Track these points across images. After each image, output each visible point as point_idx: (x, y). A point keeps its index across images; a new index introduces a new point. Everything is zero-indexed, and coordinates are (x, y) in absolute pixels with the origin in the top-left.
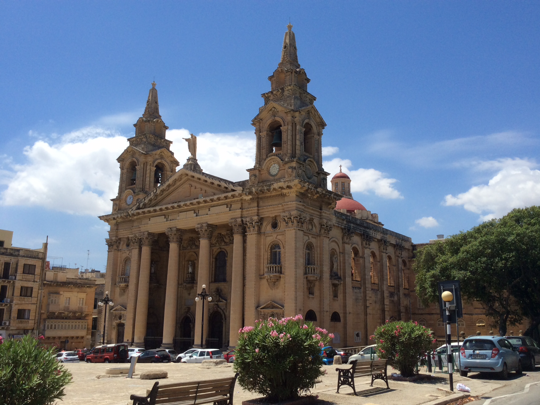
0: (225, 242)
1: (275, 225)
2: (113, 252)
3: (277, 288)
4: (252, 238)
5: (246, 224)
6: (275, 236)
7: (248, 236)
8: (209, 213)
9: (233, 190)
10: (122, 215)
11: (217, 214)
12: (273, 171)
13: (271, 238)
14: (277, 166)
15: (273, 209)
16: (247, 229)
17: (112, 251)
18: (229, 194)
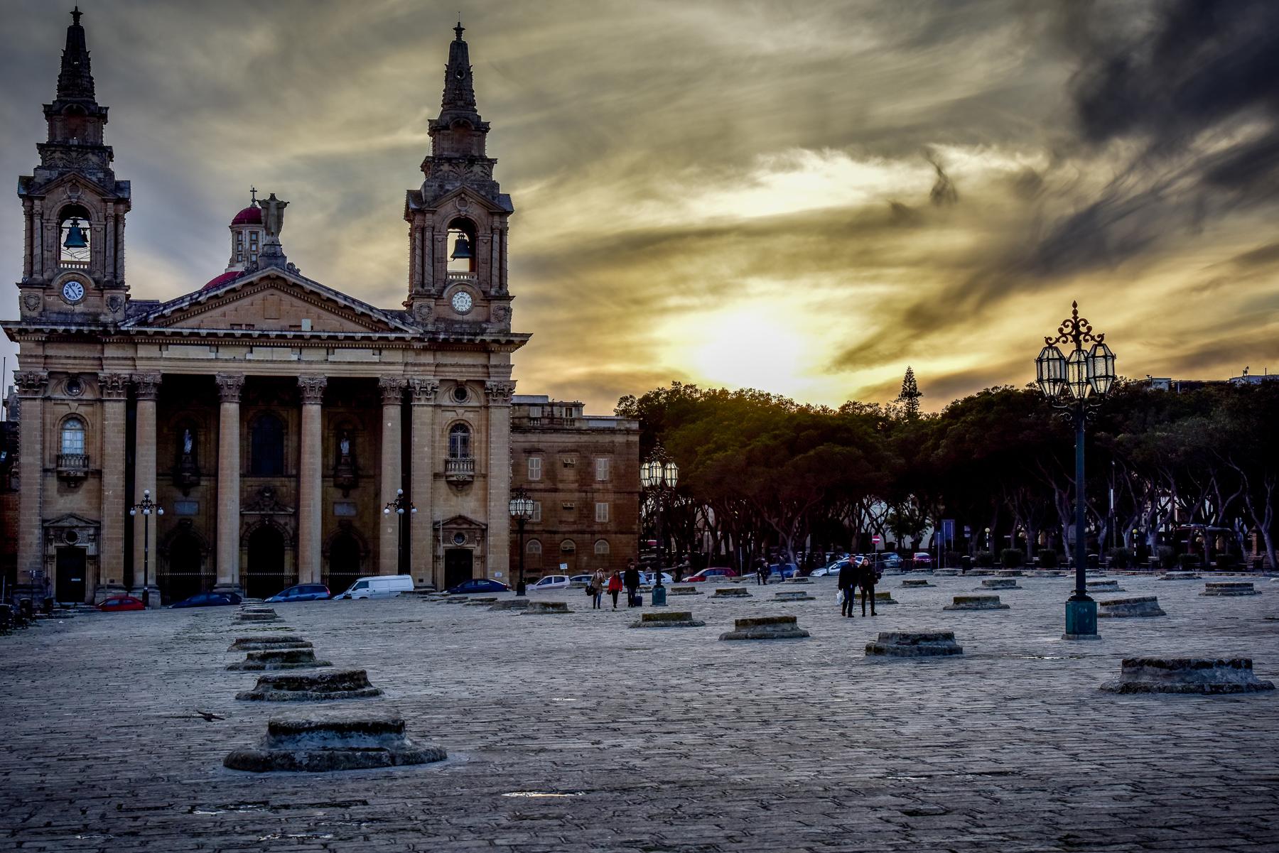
1: (461, 393)
2: (38, 402)
3: (467, 495)
4: (422, 414)
5: (414, 388)
6: (460, 411)
7: (415, 409)
8: (331, 358)
9: (401, 331)
10: (85, 329)
12: (460, 304)
13: (454, 413)
14: (467, 296)
15: (464, 369)
16: (415, 396)
17: (35, 399)
18: (393, 335)
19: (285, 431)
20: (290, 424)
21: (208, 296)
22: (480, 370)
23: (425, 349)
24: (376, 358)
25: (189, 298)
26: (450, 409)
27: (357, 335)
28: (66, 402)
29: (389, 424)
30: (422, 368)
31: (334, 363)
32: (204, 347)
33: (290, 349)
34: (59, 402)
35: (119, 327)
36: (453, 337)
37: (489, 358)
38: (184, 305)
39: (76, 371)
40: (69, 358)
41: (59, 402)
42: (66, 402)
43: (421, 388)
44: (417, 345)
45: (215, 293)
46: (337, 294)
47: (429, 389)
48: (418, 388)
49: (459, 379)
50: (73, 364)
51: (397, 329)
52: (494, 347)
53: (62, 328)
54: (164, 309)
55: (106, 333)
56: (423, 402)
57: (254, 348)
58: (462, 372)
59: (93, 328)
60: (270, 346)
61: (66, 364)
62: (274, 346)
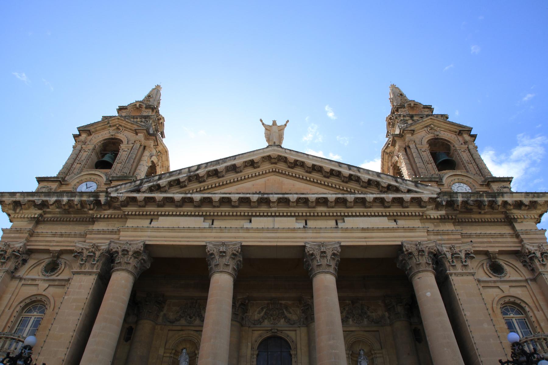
0: (285, 318)
6: (505, 287)
11: (363, 230)
13: (497, 290)
15: (491, 240)
16: (447, 264)
19: (292, 352)
20: (299, 346)
21: (207, 170)
22: (509, 240)
23: (443, 219)
24: (392, 224)
25: (187, 170)
26: (490, 284)
27: (368, 196)
28: (37, 282)
29: (429, 294)
30: (446, 237)
31: (347, 229)
32: (198, 218)
33: (294, 219)
34: (30, 282)
35: (110, 193)
36: (472, 199)
37: (513, 228)
38: (180, 176)
39: (58, 249)
40: (54, 235)
41: (30, 282)
42: (37, 282)
43: (452, 255)
44: (435, 214)
45: (215, 168)
46: (340, 164)
47: (463, 255)
48: (449, 256)
49: (490, 250)
50: (57, 242)
51: (409, 191)
52: (517, 213)
53: (54, 199)
54: (160, 179)
55: (98, 203)
56: (460, 271)
57: (253, 219)
58: (490, 242)
59: (84, 198)
60: (271, 216)
61: (50, 241)
62: (275, 216)
